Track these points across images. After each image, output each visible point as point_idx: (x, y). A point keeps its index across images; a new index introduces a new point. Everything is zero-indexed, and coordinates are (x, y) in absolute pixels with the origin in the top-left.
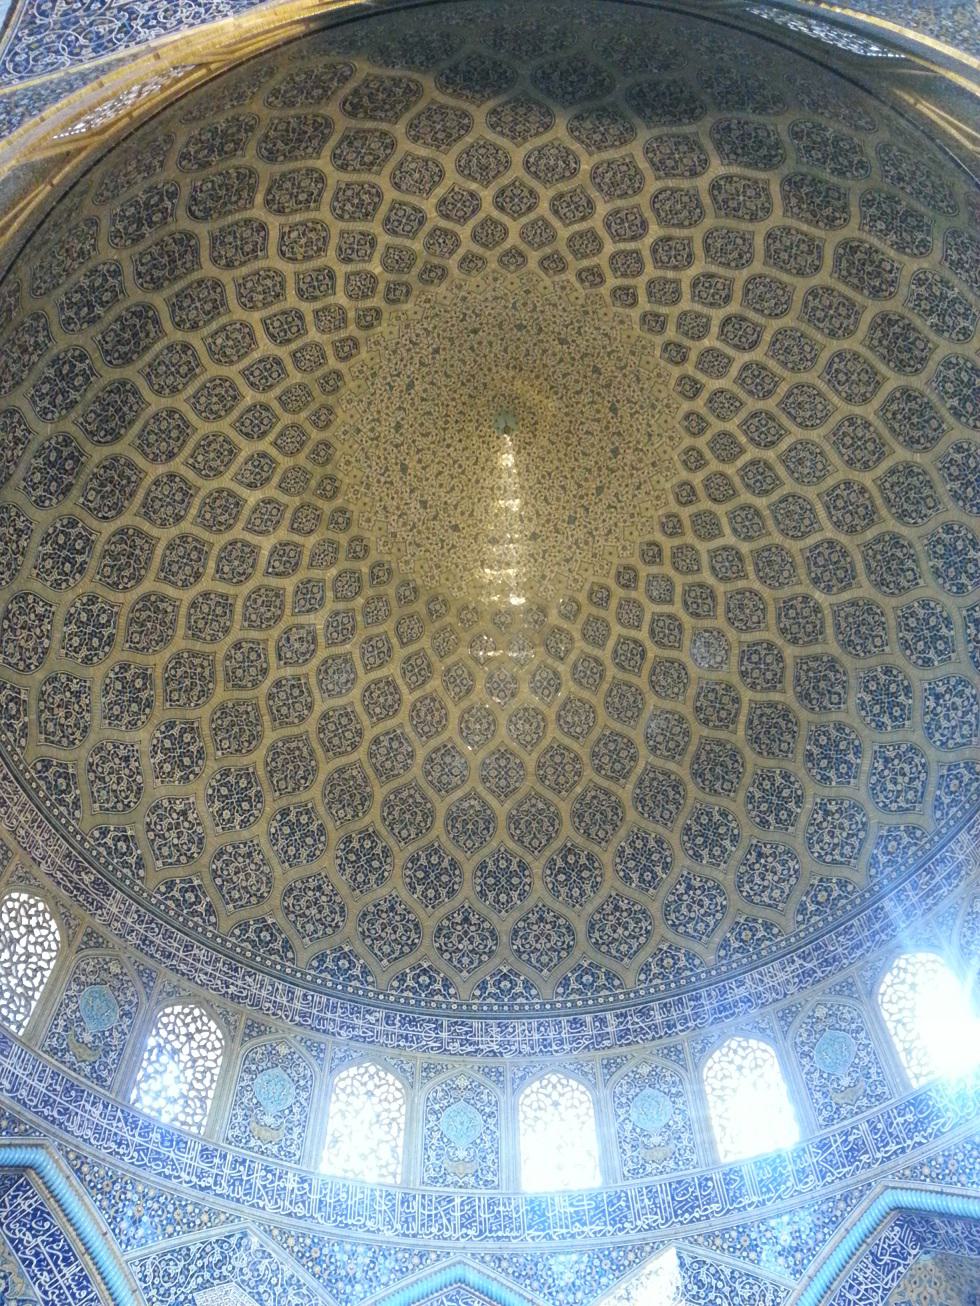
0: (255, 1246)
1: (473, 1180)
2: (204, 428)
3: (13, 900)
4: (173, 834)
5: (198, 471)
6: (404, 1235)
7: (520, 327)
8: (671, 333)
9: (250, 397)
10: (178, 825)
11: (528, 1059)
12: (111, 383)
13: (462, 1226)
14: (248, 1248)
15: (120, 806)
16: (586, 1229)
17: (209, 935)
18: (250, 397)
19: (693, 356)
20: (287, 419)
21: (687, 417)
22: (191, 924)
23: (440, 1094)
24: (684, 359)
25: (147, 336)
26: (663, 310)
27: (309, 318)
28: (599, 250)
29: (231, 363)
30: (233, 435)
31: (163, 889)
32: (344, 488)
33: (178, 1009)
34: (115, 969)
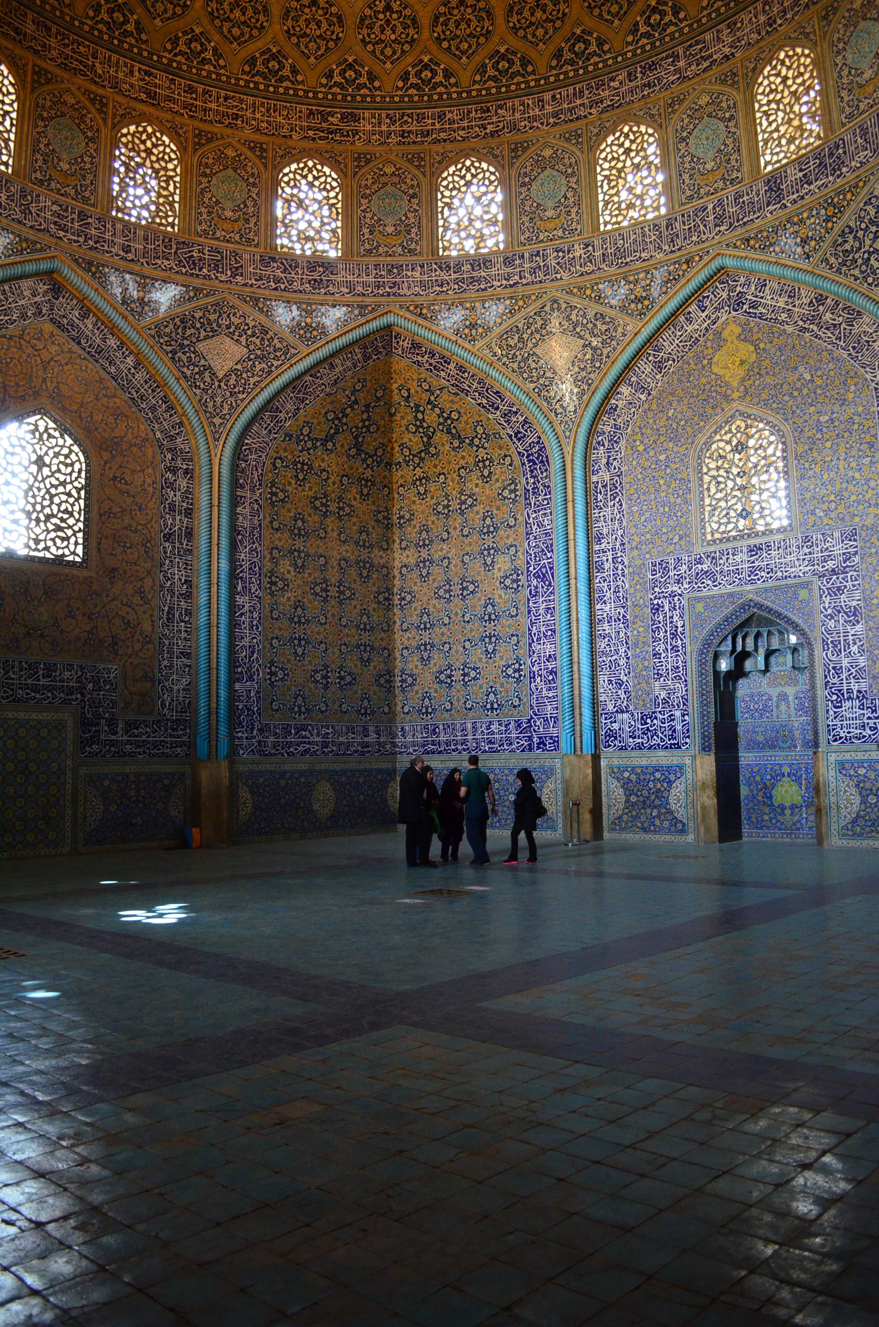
0: (564, 306)
1: (721, 183)
3: (287, 174)
4: (388, 32)
6: (672, 252)
10: (388, 22)
11: (757, 47)
13: (716, 226)
14: (559, 309)
15: (331, 44)
16: (812, 187)
17: (455, 96)
22: (436, 97)
23: (686, 121)
31: (400, 84)
33: (452, 169)
34: (389, 170)
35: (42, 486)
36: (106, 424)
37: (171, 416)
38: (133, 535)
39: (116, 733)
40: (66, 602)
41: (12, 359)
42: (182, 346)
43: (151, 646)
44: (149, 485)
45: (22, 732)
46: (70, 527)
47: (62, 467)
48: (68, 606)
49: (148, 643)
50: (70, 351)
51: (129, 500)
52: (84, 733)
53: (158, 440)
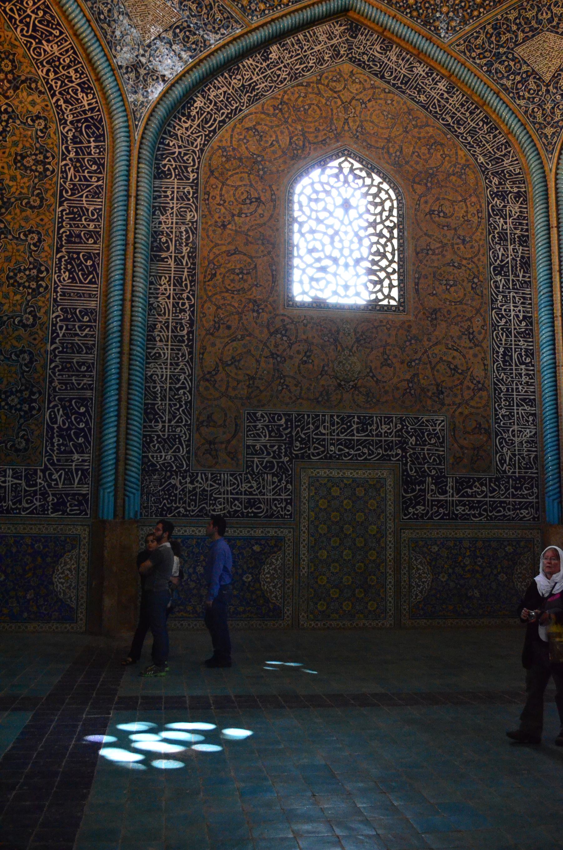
35: (349, 229)
36: (419, 156)
37: (495, 137)
38: (455, 271)
39: (445, 492)
40: (381, 350)
41: (310, 105)
42: (498, 55)
43: (484, 394)
44: (473, 215)
45: (335, 492)
46: (382, 269)
47: (371, 208)
48: (384, 353)
49: (480, 389)
50: (373, 87)
51: (450, 234)
52: (406, 491)
53: (481, 165)
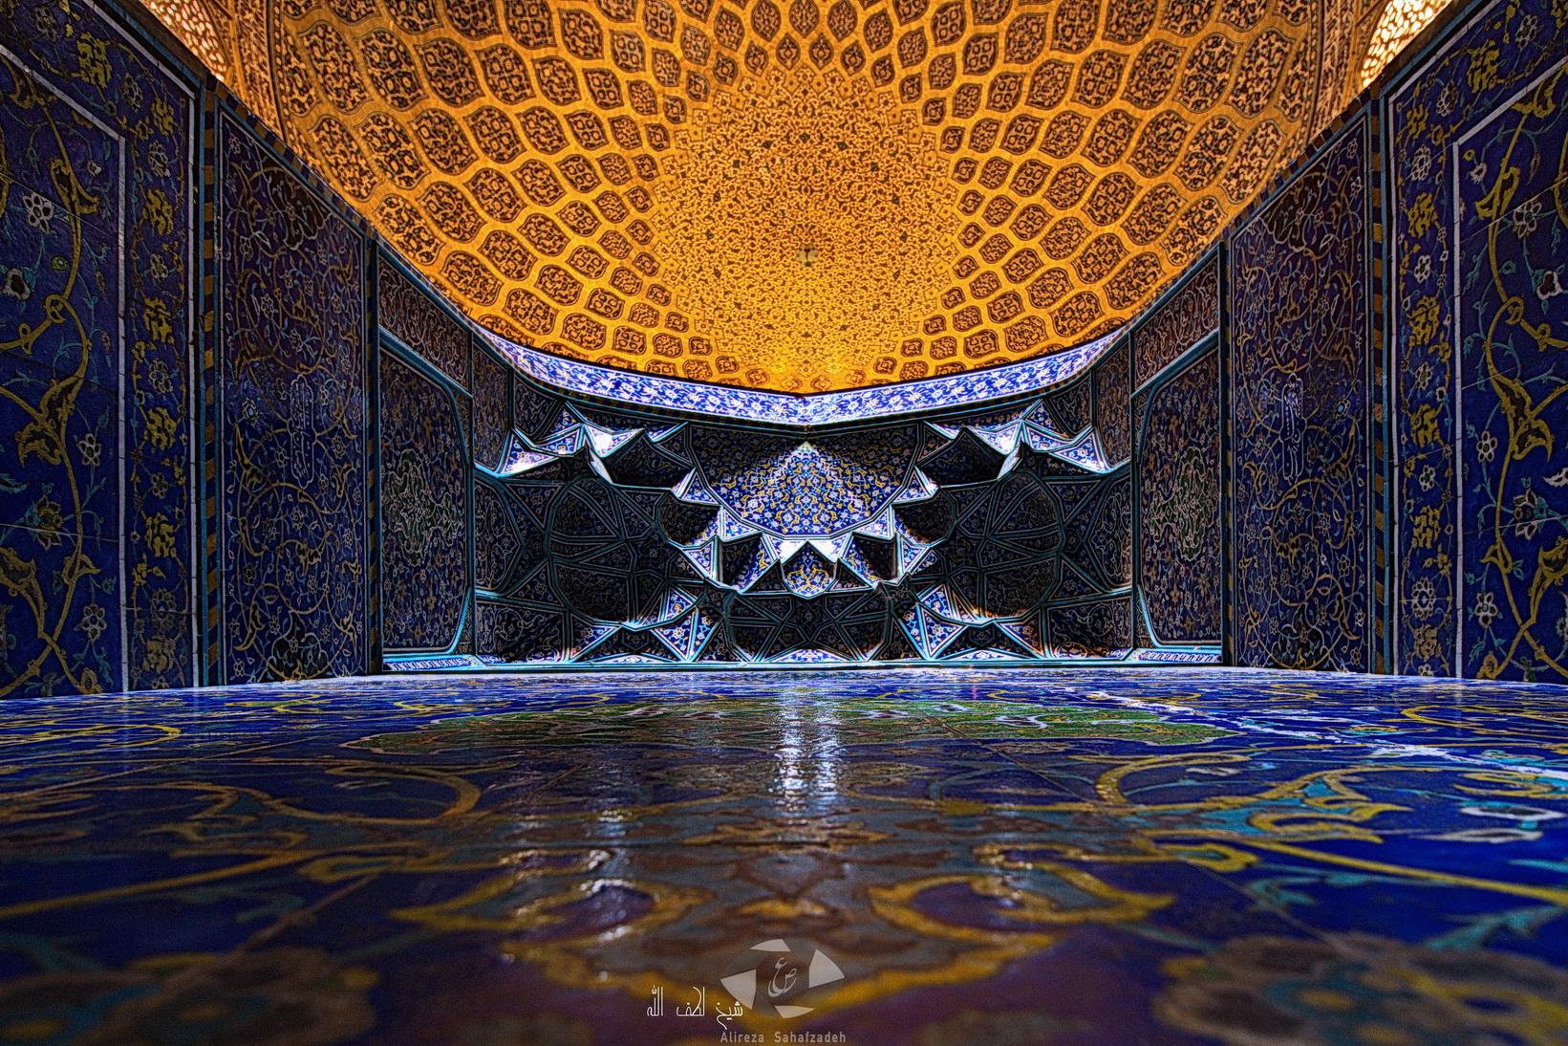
2: (532, 154)
5: (527, 191)
7: (805, 138)
8: (928, 92)
9: (573, 147)
12: (452, 43)
18: (573, 147)
19: (949, 107)
20: (606, 186)
21: (957, 169)
24: (942, 114)
25: (485, 18)
26: (915, 70)
27: (624, 88)
28: (855, 23)
29: (557, 102)
30: (558, 174)
32: (661, 270)
